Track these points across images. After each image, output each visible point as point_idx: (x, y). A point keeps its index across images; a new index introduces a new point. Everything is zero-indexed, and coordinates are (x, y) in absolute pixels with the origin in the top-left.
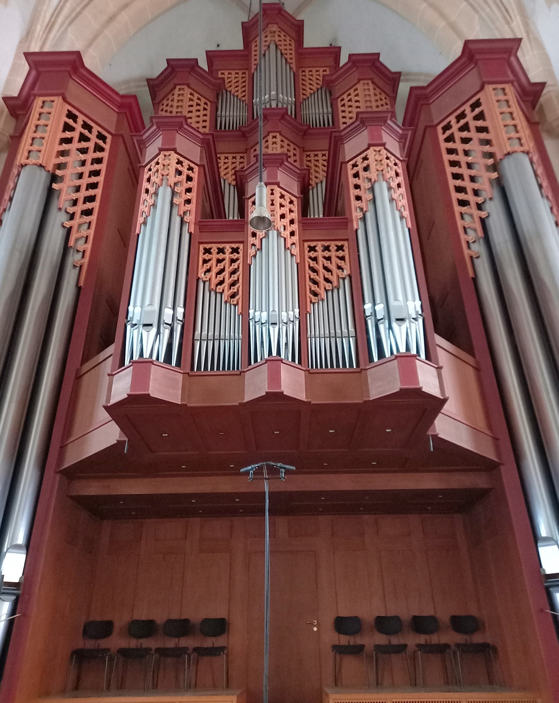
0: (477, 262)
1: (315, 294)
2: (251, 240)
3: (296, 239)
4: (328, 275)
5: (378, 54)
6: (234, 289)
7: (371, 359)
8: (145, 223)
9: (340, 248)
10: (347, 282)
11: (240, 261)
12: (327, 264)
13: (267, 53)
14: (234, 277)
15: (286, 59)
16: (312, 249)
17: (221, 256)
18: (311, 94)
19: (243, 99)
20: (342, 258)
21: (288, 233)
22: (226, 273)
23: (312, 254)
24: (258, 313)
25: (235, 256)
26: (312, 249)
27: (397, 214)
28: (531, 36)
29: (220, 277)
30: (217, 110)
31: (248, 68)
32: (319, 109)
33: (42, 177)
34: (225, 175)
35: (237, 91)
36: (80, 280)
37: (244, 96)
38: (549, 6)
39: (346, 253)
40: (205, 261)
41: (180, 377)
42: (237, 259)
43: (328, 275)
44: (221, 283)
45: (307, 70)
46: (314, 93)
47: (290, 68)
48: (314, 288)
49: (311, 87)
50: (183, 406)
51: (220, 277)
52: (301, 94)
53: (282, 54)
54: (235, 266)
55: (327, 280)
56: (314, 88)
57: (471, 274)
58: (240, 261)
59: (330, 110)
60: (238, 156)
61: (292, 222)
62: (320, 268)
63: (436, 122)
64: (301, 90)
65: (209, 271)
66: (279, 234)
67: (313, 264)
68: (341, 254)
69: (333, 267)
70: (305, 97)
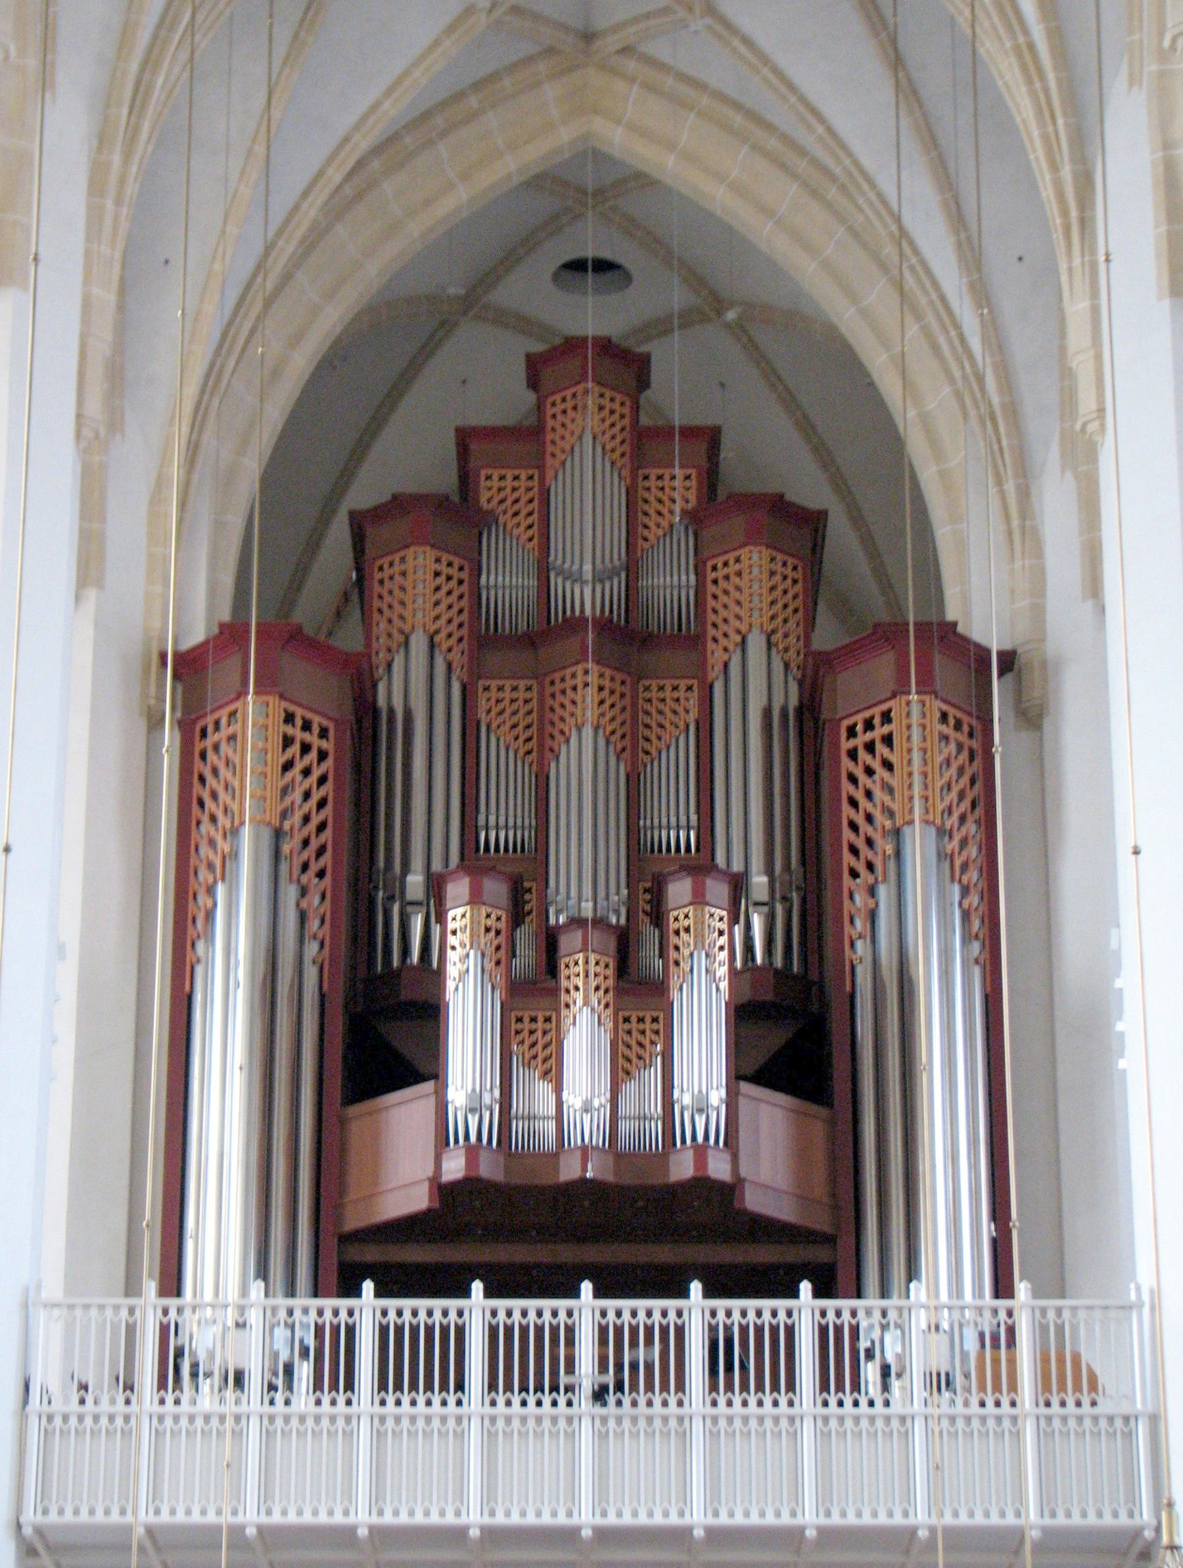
0: (859, 970)
1: (628, 1073)
2: (564, 1012)
3: (610, 1011)
4: (641, 1052)
5: (781, 496)
6: (547, 1065)
7: (674, 1144)
8: (457, 989)
9: (655, 1020)
10: (659, 1058)
11: (553, 1033)
12: (641, 1038)
13: (577, 449)
14: (548, 1052)
15: (613, 463)
16: (627, 1020)
17: (533, 1026)
18: (658, 539)
19: (530, 545)
20: (657, 1032)
21: (602, 1006)
22: (539, 1046)
23: (627, 1026)
24: (572, 1096)
25: (548, 1026)
26: (627, 1020)
27: (714, 986)
28: (1028, 523)
29: (533, 1051)
30: (479, 575)
31: (541, 468)
32: (672, 576)
33: (266, 835)
34: (499, 727)
35: (518, 525)
36: (280, 940)
37: (530, 540)
38: (1063, 472)
39: (661, 1026)
40: (517, 1032)
41: (501, 1159)
42: (551, 1030)
43: (641, 1052)
44: (535, 1057)
45: (654, 472)
46: (665, 535)
47: (620, 477)
48: (627, 1065)
49: (660, 520)
50: (507, 1185)
51: (533, 1051)
52: (640, 514)
53: (604, 453)
54: (548, 1038)
55: (640, 1058)
56: (665, 524)
57: (848, 988)
58: (553, 1033)
59: (692, 577)
60: (522, 684)
61: (606, 991)
62: (633, 1043)
63: (841, 714)
64: (640, 529)
65: (522, 1042)
66: (593, 1009)
67: (627, 1038)
68: (655, 1026)
69: (647, 1043)
70: (646, 545)
